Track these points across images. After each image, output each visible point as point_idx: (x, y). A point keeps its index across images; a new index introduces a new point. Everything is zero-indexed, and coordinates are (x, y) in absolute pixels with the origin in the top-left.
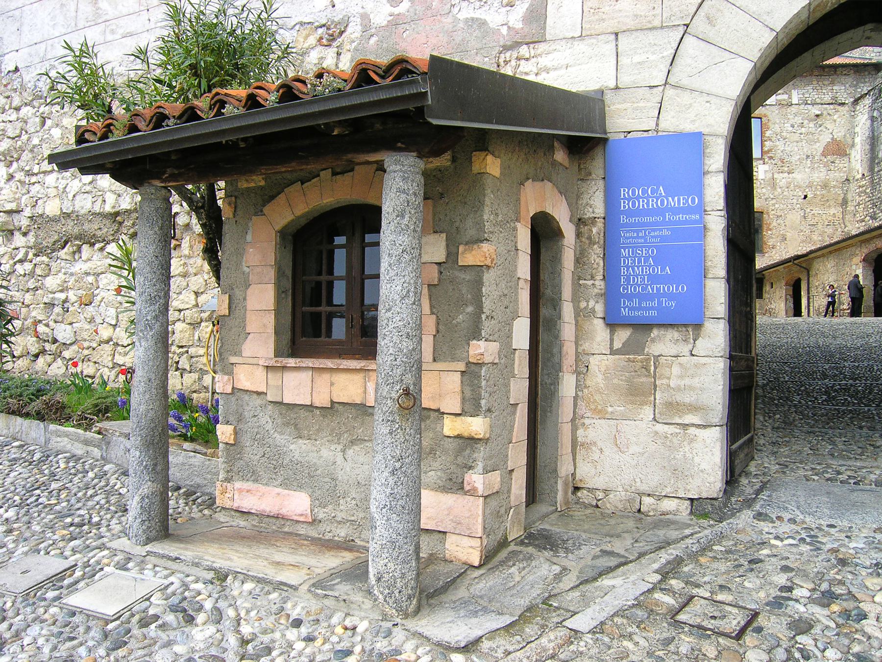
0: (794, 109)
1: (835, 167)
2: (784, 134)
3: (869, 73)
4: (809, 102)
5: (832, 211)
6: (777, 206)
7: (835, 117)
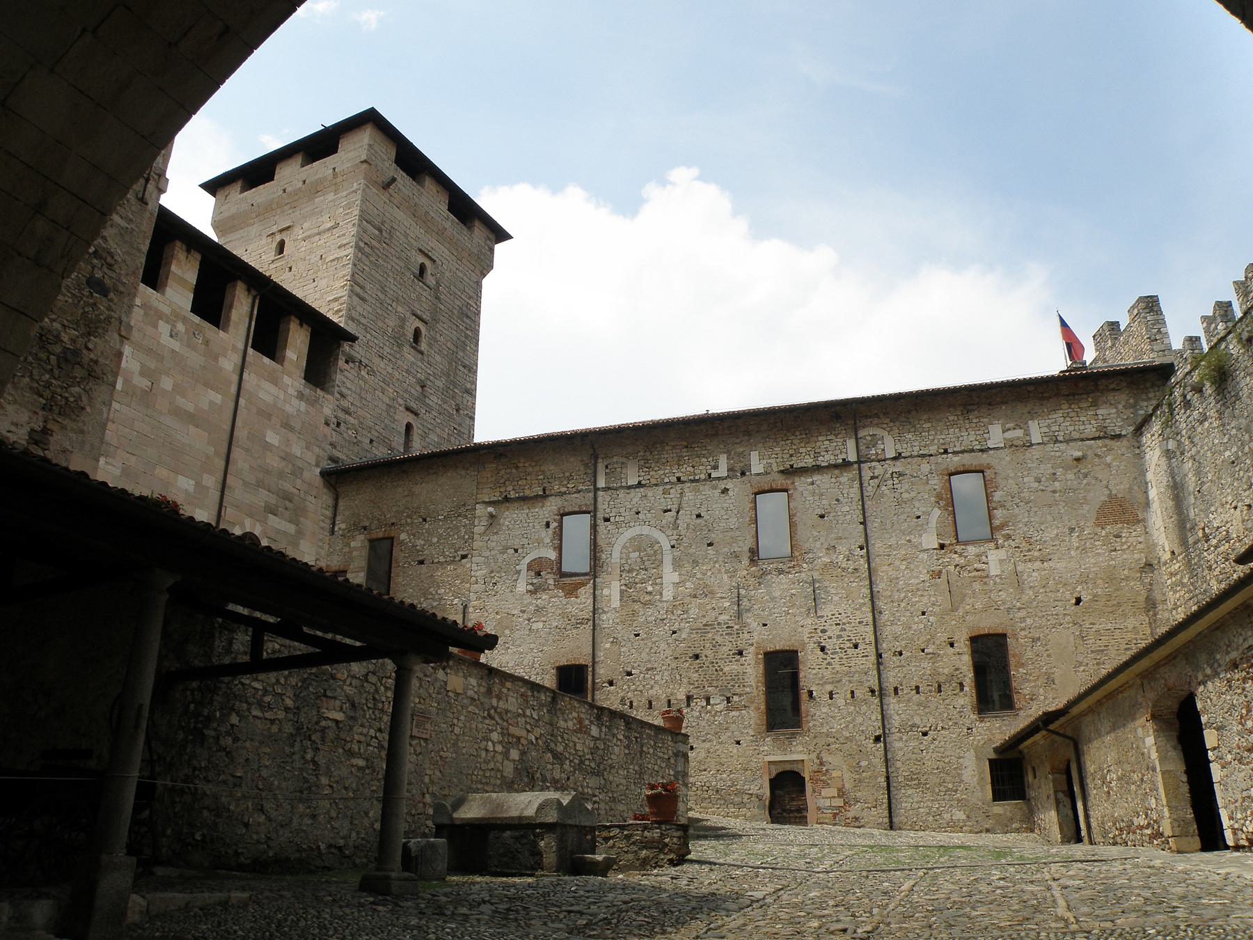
0: (1036, 452)
1: (1123, 544)
2: (1026, 495)
3: (1153, 386)
4: (1060, 438)
5: (1131, 623)
6: (1029, 621)
7: (1109, 459)
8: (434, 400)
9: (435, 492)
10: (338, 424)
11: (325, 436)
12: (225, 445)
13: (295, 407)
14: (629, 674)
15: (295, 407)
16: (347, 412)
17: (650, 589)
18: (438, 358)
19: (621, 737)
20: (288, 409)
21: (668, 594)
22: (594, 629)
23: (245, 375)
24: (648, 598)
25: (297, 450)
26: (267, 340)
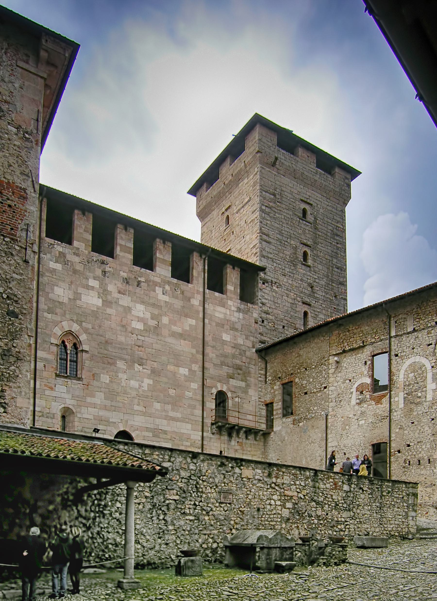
8: (320, 294)
9: (309, 352)
10: (263, 321)
14: (409, 446)
16: (267, 313)
17: (420, 394)
19: (367, 489)
20: (233, 319)
21: (429, 397)
22: (390, 422)
23: (206, 306)
24: (418, 400)
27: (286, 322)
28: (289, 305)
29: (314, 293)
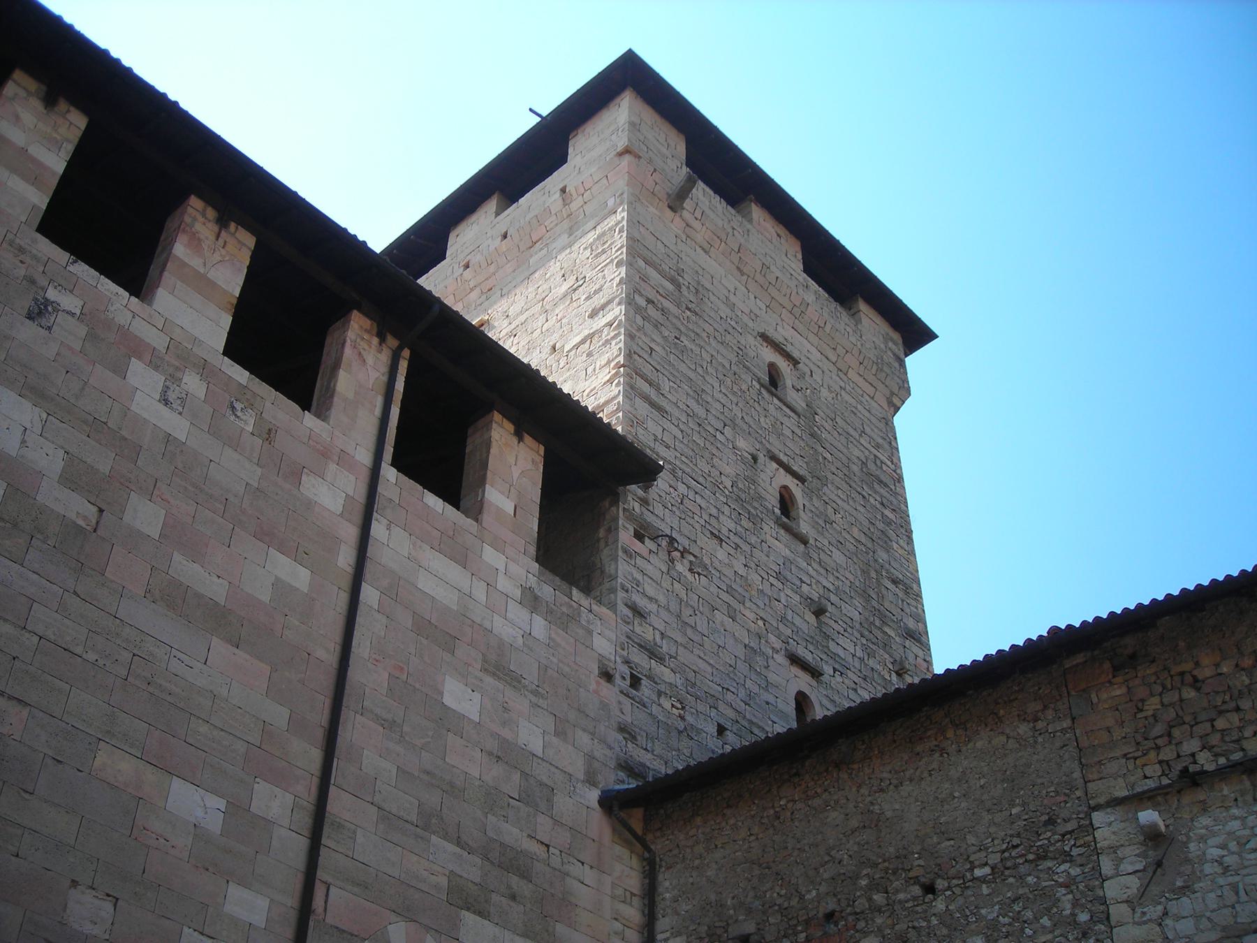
10: (635, 682)
11: (604, 706)
12: (324, 703)
13: (515, 624)
15: (515, 624)
16: (652, 652)
18: (837, 555)
23: (378, 529)
25: (531, 735)
26: (432, 448)
27: (730, 713)
28: (740, 652)
29: (827, 637)
